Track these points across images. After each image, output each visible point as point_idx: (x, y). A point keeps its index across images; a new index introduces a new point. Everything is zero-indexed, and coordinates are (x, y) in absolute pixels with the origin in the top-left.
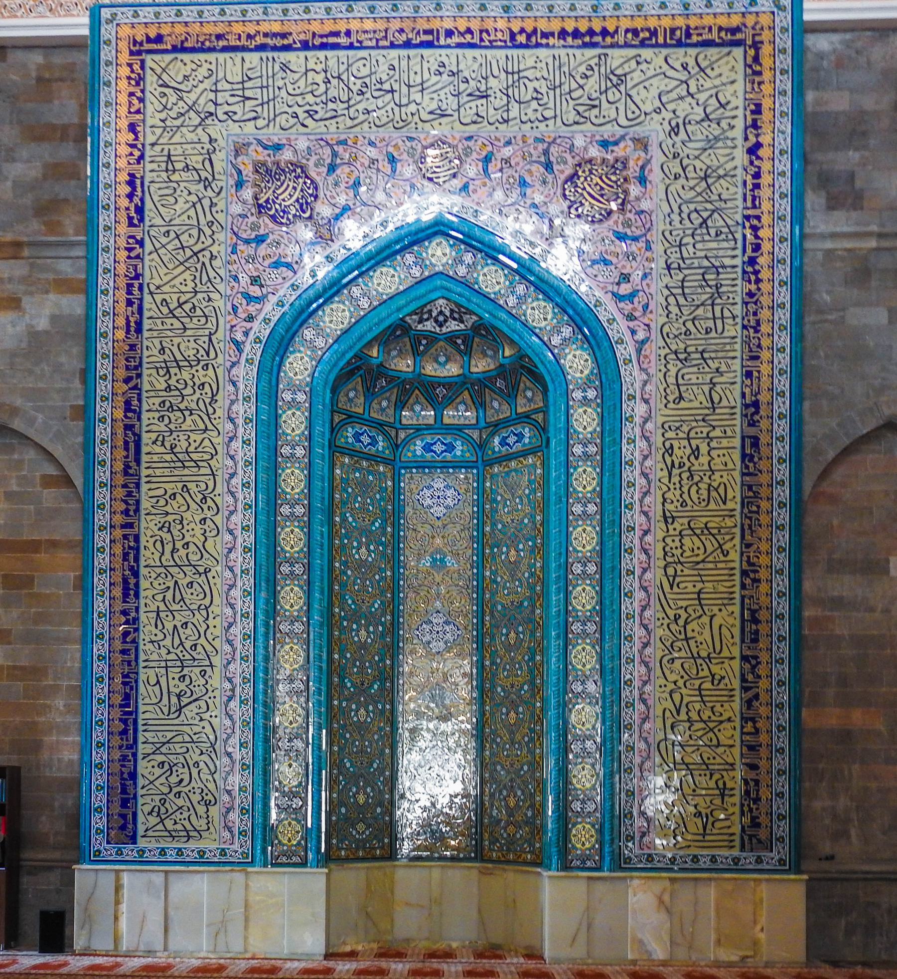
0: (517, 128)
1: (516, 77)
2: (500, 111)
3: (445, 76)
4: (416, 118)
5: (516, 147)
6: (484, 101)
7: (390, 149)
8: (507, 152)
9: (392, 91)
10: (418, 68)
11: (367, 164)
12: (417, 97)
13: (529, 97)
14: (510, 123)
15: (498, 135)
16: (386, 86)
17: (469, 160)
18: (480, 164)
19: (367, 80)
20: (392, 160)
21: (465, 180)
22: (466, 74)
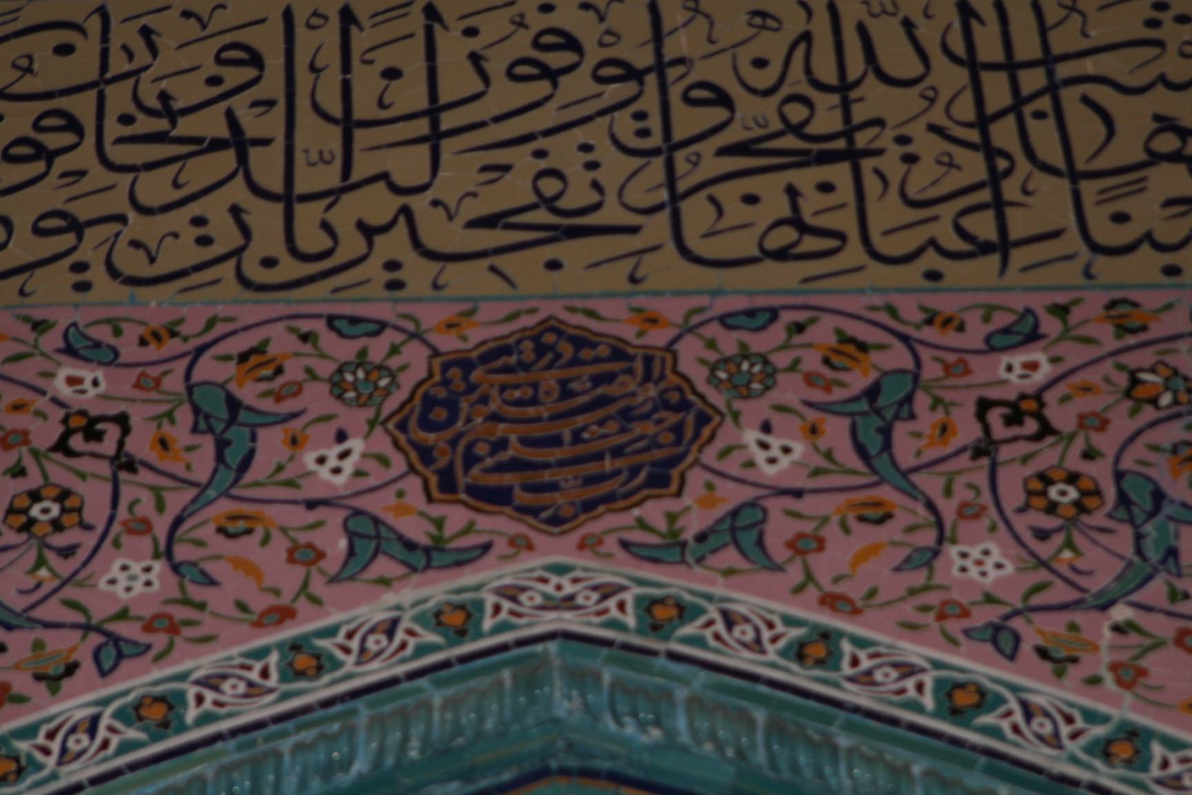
0: (1070, 273)
1: (1032, 80)
2: (947, 211)
3: (577, 84)
4: (395, 244)
5: (1075, 354)
6: (840, 173)
7: (207, 369)
8: (1015, 372)
9: (239, 142)
10: (411, 59)
11: (46, 432)
12: (410, 165)
13: (1127, 149)
14: (1019, 257)
15: (945, 303)
16: (211, 124)
17: (758, 409)
18: (836, 431)
19: (82, 107)
20: (225, 422)
21: (732, 495)
22: (718, 72)
